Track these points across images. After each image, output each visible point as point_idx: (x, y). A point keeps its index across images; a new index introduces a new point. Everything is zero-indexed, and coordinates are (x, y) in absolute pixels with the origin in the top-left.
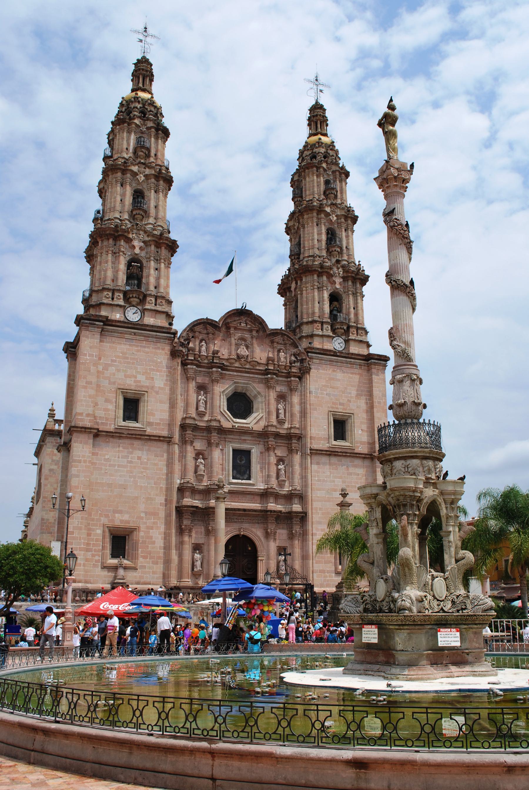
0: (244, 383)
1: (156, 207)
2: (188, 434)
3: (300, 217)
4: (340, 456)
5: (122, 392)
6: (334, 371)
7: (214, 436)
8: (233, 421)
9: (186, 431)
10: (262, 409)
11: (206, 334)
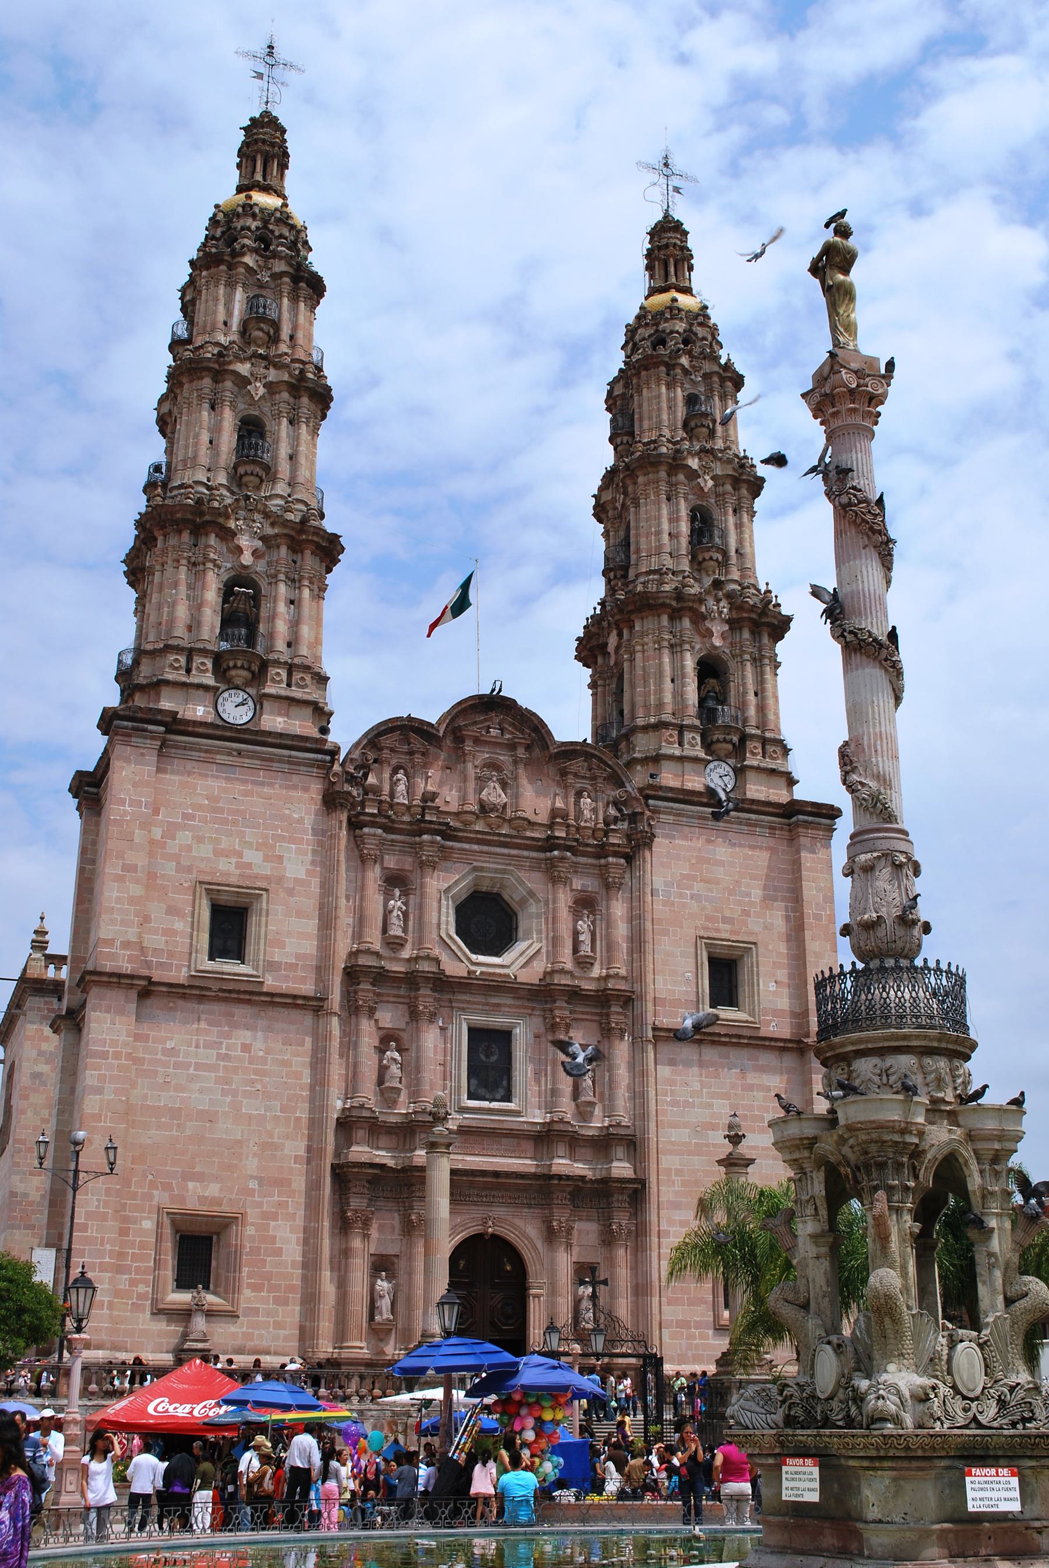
0: (496, 871)
1: (291, 458)
2: (363, 990)
3: (628, 482)
4: (725, 1044)
5: (206, 889)
6: (709, 841)
7: (425, 996)
8: (469, 959)
9: (359, 984)
10: (539, 932)
11: (406, 753)
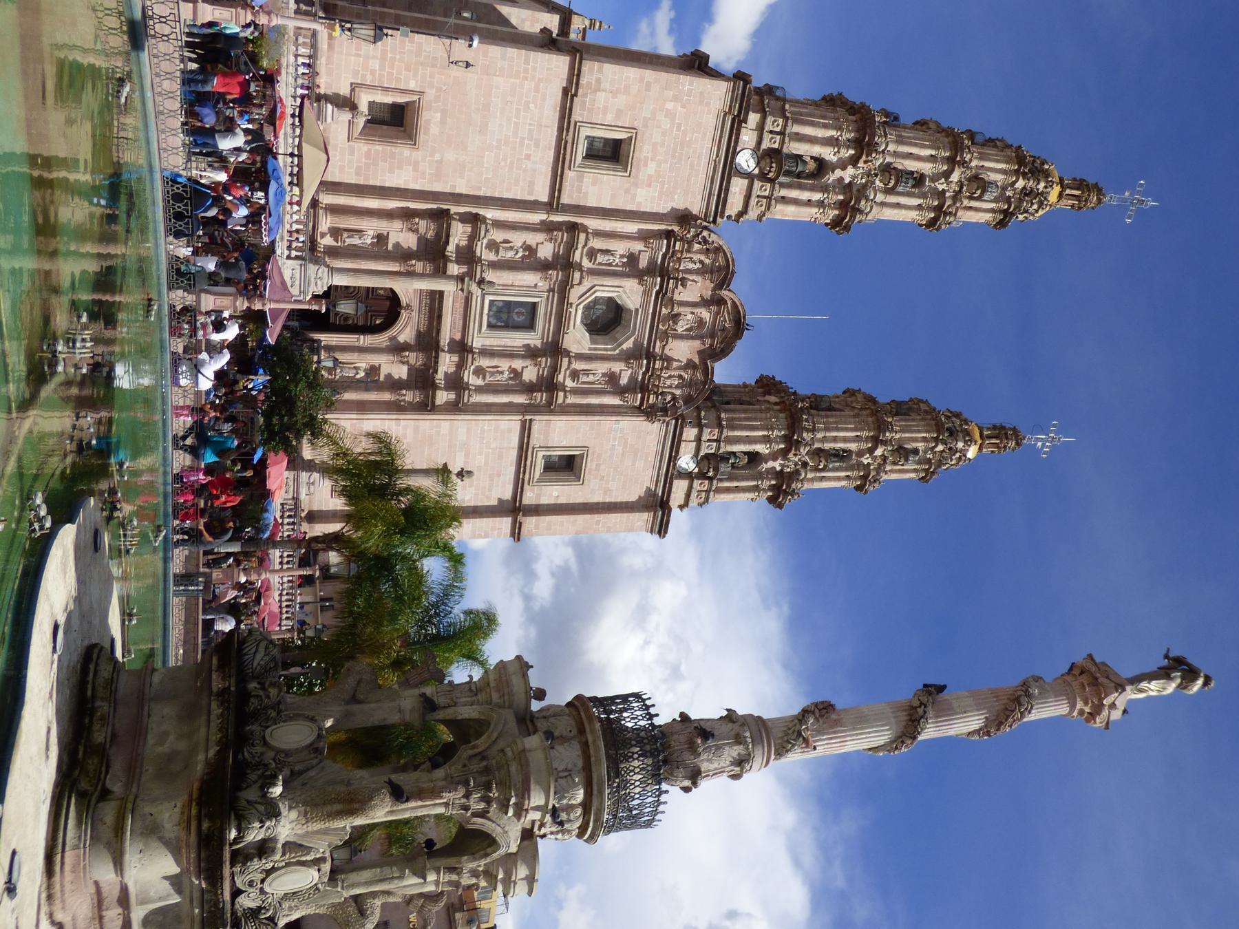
1: (898, 204)
5: (631, 137)
